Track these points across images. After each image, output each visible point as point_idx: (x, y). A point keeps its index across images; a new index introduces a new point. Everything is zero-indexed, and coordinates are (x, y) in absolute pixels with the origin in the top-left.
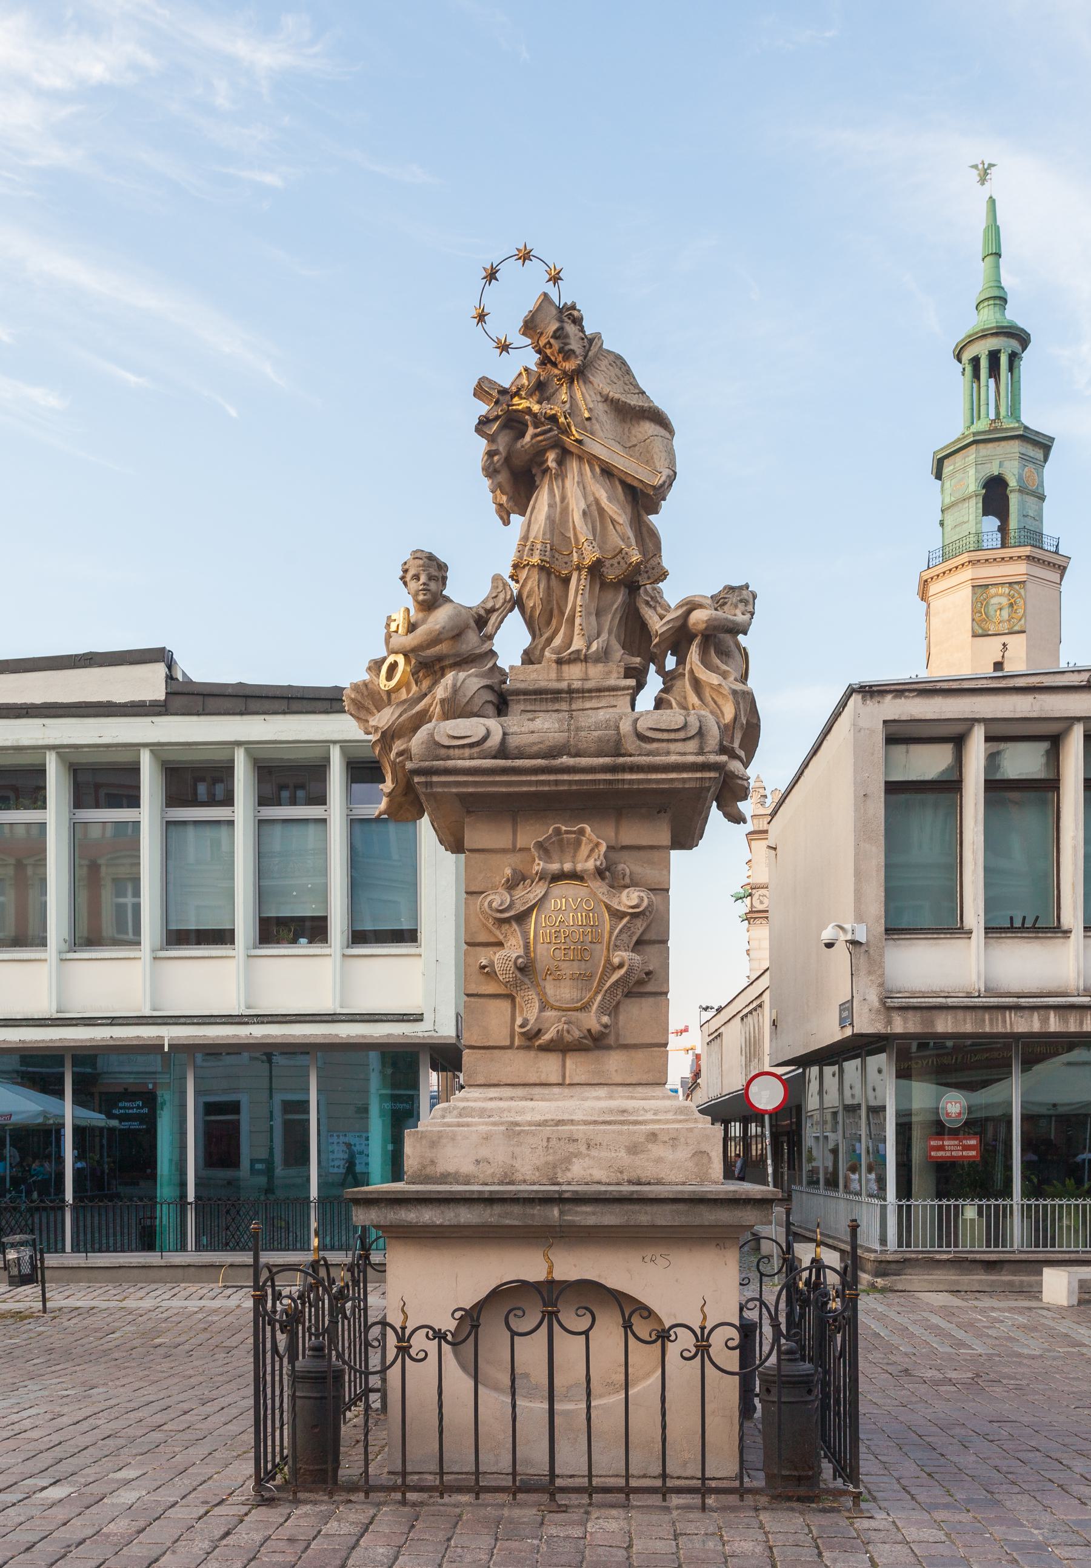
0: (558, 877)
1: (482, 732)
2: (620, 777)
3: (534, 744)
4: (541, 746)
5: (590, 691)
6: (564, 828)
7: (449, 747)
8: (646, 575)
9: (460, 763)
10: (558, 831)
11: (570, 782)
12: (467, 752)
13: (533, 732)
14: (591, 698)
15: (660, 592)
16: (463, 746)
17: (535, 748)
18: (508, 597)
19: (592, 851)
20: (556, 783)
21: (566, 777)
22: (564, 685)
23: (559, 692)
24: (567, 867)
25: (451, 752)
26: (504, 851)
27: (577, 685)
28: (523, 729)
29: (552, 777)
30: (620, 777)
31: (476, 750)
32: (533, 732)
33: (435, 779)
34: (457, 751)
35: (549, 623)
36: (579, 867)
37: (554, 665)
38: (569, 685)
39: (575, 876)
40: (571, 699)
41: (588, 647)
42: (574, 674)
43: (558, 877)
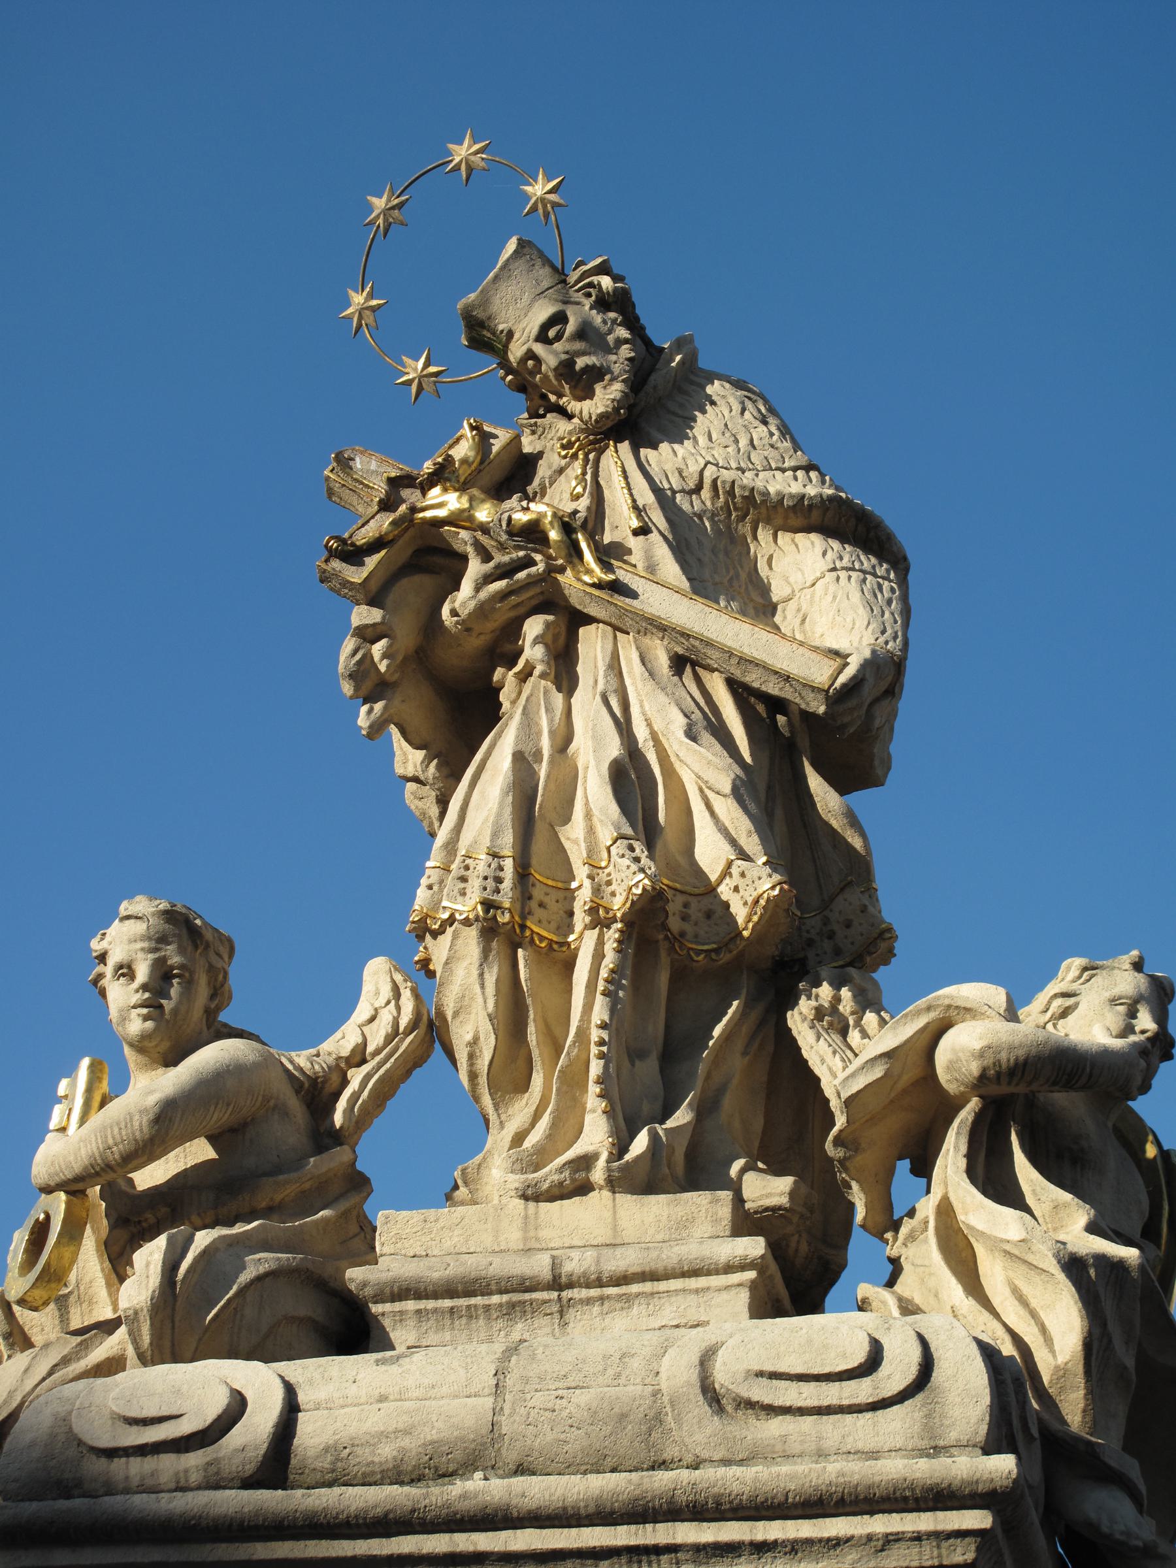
1: (215, 1404)
3: (383, 1436)
5: (623, 1280)
7: (112, 1453)
8: (827, 945)
13: (383, 1399)
14: (629, 1299)
15: (875, 983)
17: (386, 1452)
18: (404, 1022)
22: (540, 1266)
23: (527, 1285)
28: (353, 1390)
31: (194, 1460)
32: (383, 1399)
38: (555, 1264)
41: (621, 1148)
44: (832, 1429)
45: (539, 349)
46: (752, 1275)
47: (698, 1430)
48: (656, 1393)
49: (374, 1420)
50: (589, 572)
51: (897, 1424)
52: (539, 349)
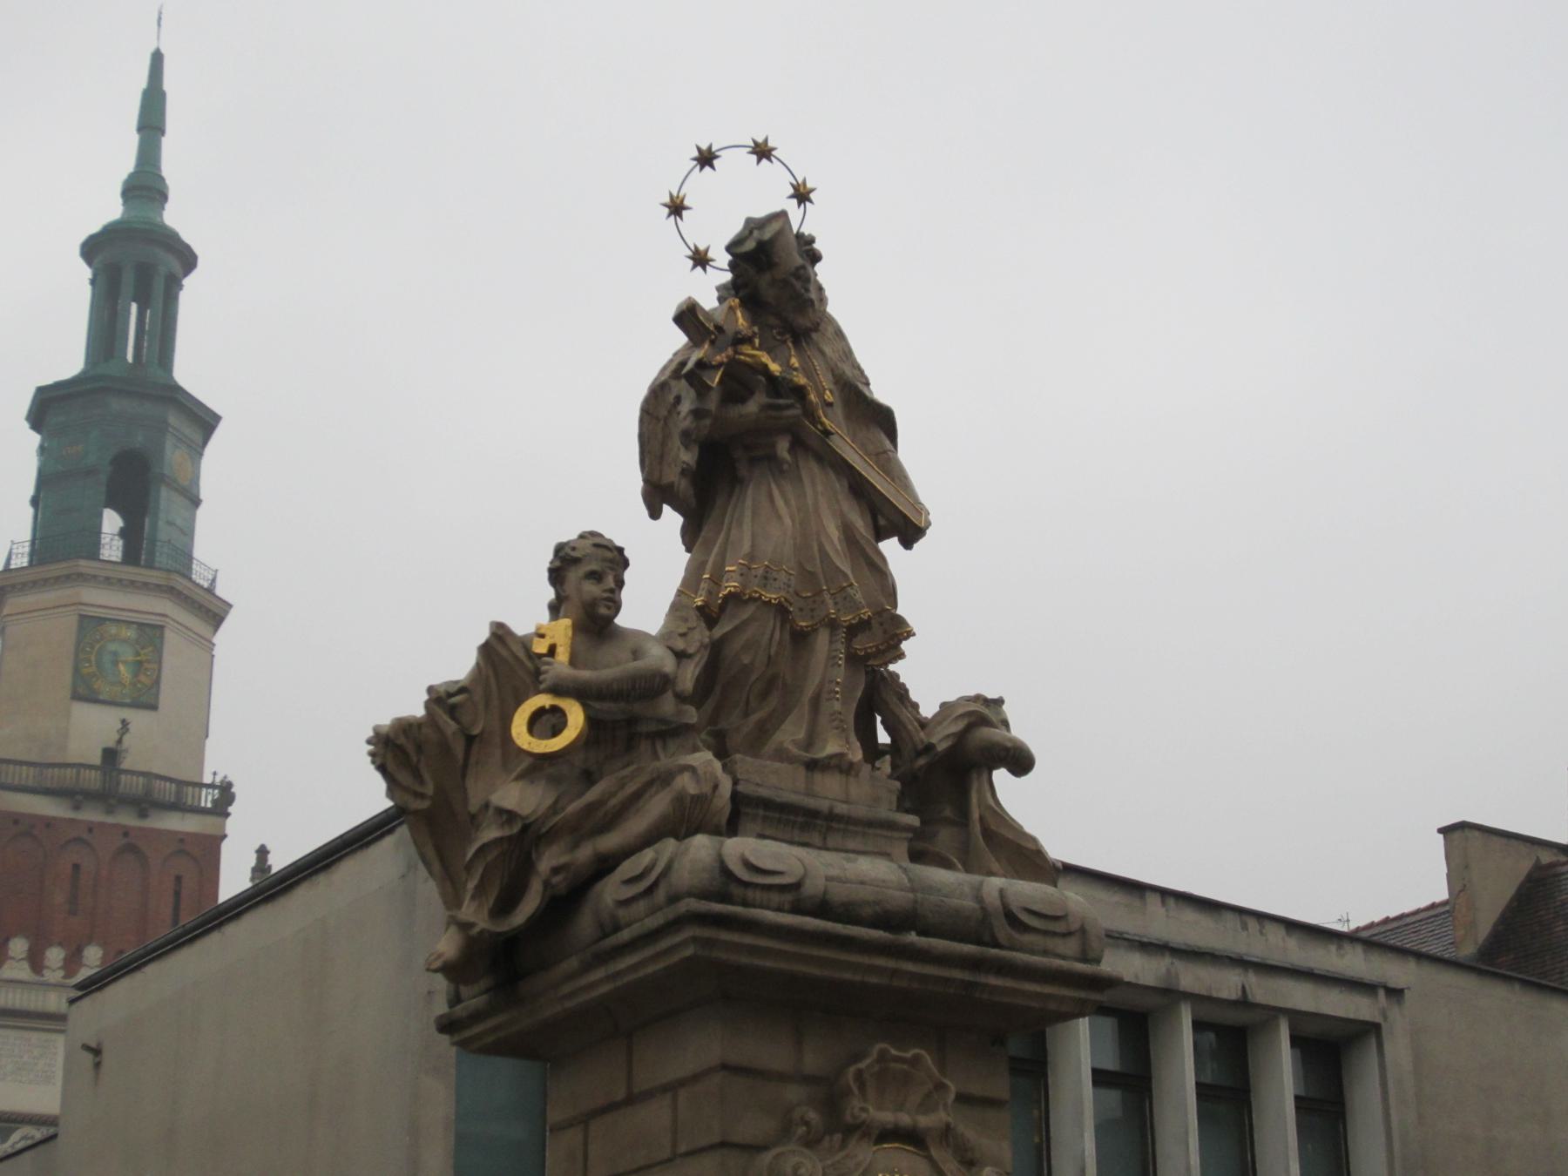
0: (888, 1135)
1: (799, 871)
2: (983, 979)
4: (877, 908)
6: (894, 1052)
7: (747, 885)
9: (770, 916)
10: (883, 1056)
11: (912, 975)
12: (776, 898)
16: (769, 888)
19: (928, 1095)
20: (895, 973)
21: (910, 967)
22: (824, 805)
24: (905, 1119)
25: (750, 894)
26: (782, 1077)
27: (841, 808)
29: (890, 963)
30: (983, 979)
31: (788, 897)
32: (862, 883)
33: (726, 936)
34: (758, 896)
35: (764, 695)
36: (924, 1121)
37: (802, 771)
39: (913, 1138)
40: (829, 829)
42: (829, 791)
43: (888, 1135)
44: (1051, 943)
45: (794, 281)
46: (910, 835)
47: (1003, 931)
48: (983, 909)
49: (864, 893)
50: (822, 424)
51: (1070, 946)
52: (794, 281)
